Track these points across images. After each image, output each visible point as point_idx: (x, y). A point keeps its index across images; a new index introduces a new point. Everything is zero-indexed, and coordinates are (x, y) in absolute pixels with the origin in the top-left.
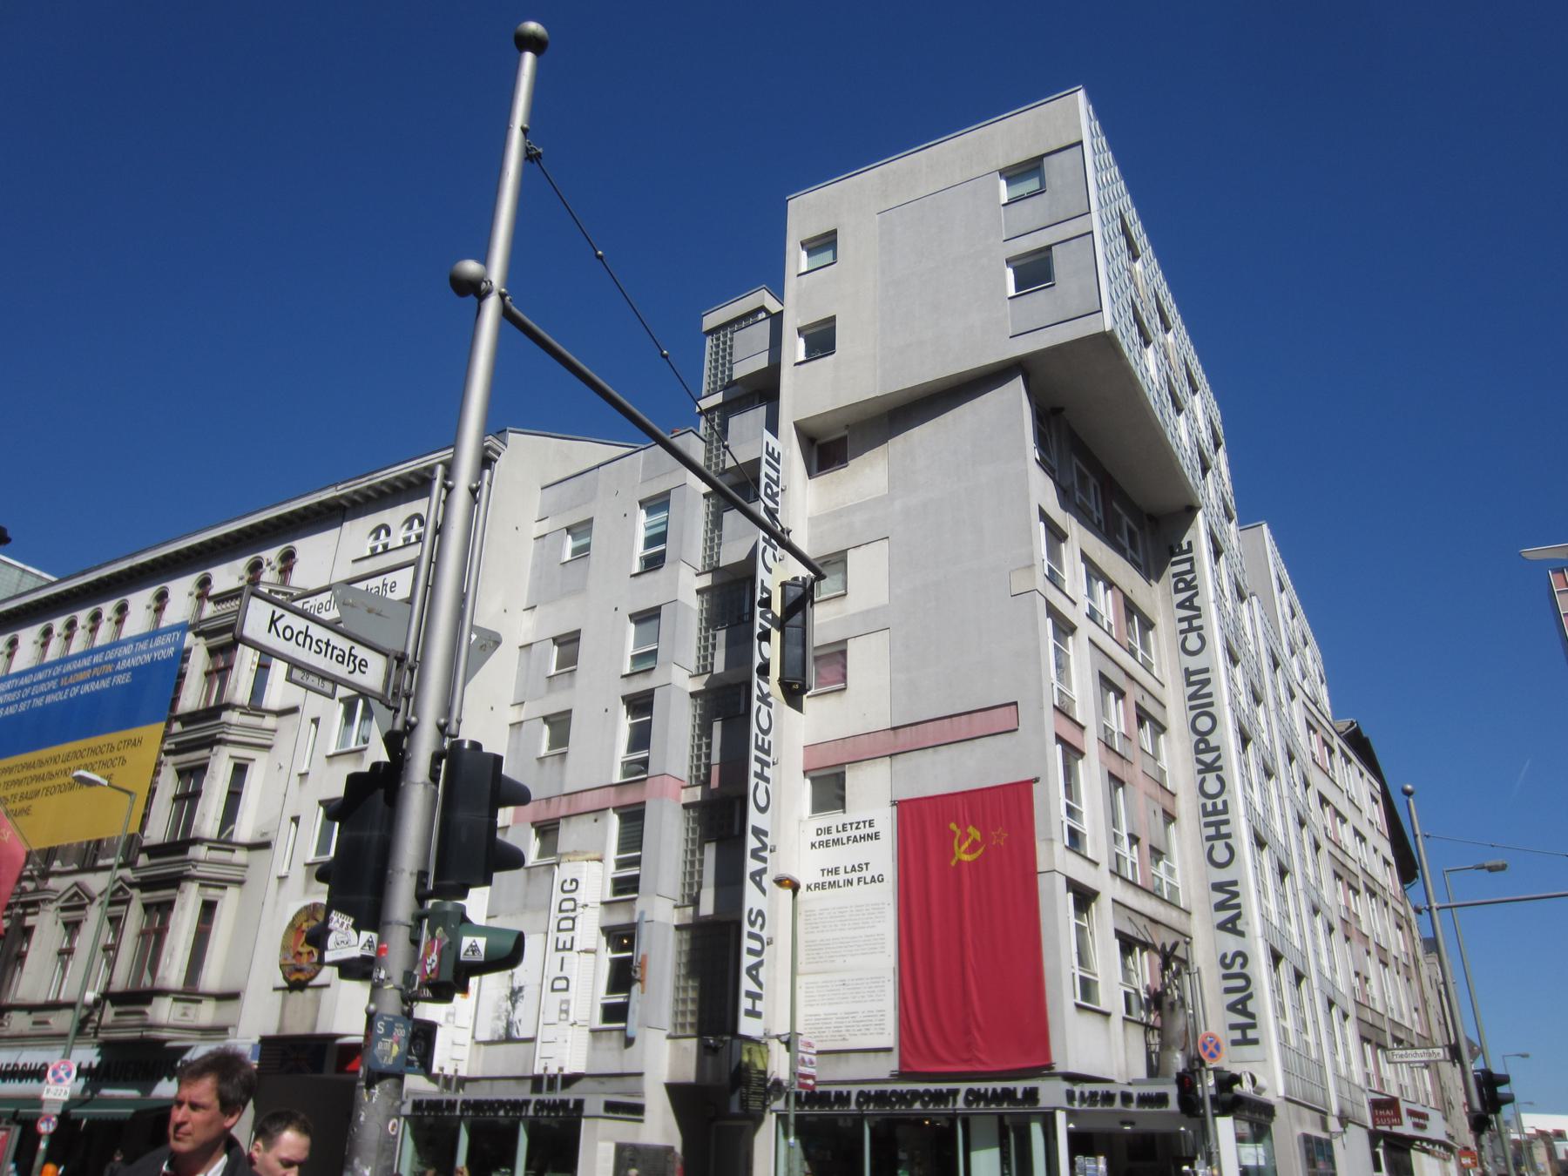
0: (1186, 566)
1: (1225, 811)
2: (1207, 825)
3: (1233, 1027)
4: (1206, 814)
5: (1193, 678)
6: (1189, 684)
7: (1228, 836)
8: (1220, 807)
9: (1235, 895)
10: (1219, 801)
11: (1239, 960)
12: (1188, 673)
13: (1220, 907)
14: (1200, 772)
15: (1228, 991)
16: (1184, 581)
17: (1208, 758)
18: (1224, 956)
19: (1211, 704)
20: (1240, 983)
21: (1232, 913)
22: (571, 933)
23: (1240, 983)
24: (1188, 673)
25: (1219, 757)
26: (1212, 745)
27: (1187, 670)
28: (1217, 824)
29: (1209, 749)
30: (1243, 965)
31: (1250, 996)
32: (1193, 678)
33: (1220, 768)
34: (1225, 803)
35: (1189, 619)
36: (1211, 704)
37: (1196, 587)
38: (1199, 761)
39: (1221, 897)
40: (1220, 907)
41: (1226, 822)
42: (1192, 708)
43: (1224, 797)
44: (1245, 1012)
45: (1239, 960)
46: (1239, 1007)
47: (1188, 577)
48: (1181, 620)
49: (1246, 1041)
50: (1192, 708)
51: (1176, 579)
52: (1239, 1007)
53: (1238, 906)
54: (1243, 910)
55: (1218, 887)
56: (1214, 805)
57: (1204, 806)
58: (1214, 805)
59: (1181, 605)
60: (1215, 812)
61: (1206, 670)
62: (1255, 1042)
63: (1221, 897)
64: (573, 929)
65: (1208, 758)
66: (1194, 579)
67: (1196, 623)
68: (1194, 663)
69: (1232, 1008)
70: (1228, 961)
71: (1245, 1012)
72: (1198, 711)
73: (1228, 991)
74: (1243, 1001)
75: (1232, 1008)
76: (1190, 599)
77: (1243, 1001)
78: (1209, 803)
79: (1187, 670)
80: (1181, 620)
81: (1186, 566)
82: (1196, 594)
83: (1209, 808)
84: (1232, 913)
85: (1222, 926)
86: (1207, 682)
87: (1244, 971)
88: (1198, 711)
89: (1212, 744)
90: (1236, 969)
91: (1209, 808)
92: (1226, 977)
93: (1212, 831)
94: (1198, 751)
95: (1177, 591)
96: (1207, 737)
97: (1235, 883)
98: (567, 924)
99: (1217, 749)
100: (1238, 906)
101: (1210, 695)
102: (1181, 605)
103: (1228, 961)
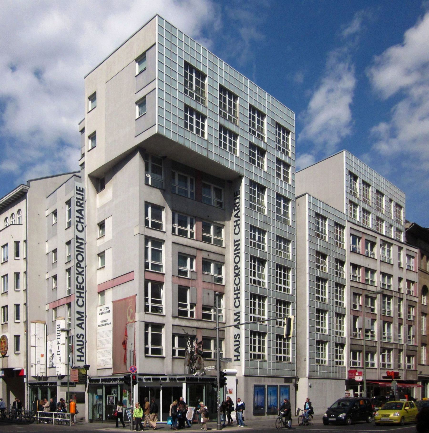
1: (239, 290)
2: (235, 294)
3: (235, 356)
4: (235, 291)
5: (236, 243)
6: (235, 246)
7: (239, 298)
9: (239, 316)
10: (238, 286)
12: (235, 241)
17: (237, 271)
18: (235, 335)
19: (239, 253)
20: (237, 343)
22: (59, 339)
23: (237, 343)
24: (235, 241)
25: (239, 271)
26: (239, 267)
30: (239, 338)
32: (236, 243)
34: (239, 287)
38: (235, 273)
39: (236, 317)
41: (239, 293)
43: (239, 285)
46: (237, 350)
47: (238, 205)
48: (235, 222)
50: (235, 254)
52: (237, 350)
55: (236, 314)
56: (237, 287)
57: (235, 288)
58: (237, 287)
61: (239, 240)
62: (239, 360)
63: (236, 317)
64: (60, 338)
65: (237, 271)
66: (239, 206)
69: (235, 350)
72: (236, 255)
74: (238, 348)
82: (239, 212)
83: (236, 289)
86: (239, 245)
88: (236, 255)
89: (239, 267)
90: (237, 339)
92: (235, 341)
94: (235, 269)
97: (239, 313)
98: (59, 337)
99: (239, 268)
101: (239, 249)
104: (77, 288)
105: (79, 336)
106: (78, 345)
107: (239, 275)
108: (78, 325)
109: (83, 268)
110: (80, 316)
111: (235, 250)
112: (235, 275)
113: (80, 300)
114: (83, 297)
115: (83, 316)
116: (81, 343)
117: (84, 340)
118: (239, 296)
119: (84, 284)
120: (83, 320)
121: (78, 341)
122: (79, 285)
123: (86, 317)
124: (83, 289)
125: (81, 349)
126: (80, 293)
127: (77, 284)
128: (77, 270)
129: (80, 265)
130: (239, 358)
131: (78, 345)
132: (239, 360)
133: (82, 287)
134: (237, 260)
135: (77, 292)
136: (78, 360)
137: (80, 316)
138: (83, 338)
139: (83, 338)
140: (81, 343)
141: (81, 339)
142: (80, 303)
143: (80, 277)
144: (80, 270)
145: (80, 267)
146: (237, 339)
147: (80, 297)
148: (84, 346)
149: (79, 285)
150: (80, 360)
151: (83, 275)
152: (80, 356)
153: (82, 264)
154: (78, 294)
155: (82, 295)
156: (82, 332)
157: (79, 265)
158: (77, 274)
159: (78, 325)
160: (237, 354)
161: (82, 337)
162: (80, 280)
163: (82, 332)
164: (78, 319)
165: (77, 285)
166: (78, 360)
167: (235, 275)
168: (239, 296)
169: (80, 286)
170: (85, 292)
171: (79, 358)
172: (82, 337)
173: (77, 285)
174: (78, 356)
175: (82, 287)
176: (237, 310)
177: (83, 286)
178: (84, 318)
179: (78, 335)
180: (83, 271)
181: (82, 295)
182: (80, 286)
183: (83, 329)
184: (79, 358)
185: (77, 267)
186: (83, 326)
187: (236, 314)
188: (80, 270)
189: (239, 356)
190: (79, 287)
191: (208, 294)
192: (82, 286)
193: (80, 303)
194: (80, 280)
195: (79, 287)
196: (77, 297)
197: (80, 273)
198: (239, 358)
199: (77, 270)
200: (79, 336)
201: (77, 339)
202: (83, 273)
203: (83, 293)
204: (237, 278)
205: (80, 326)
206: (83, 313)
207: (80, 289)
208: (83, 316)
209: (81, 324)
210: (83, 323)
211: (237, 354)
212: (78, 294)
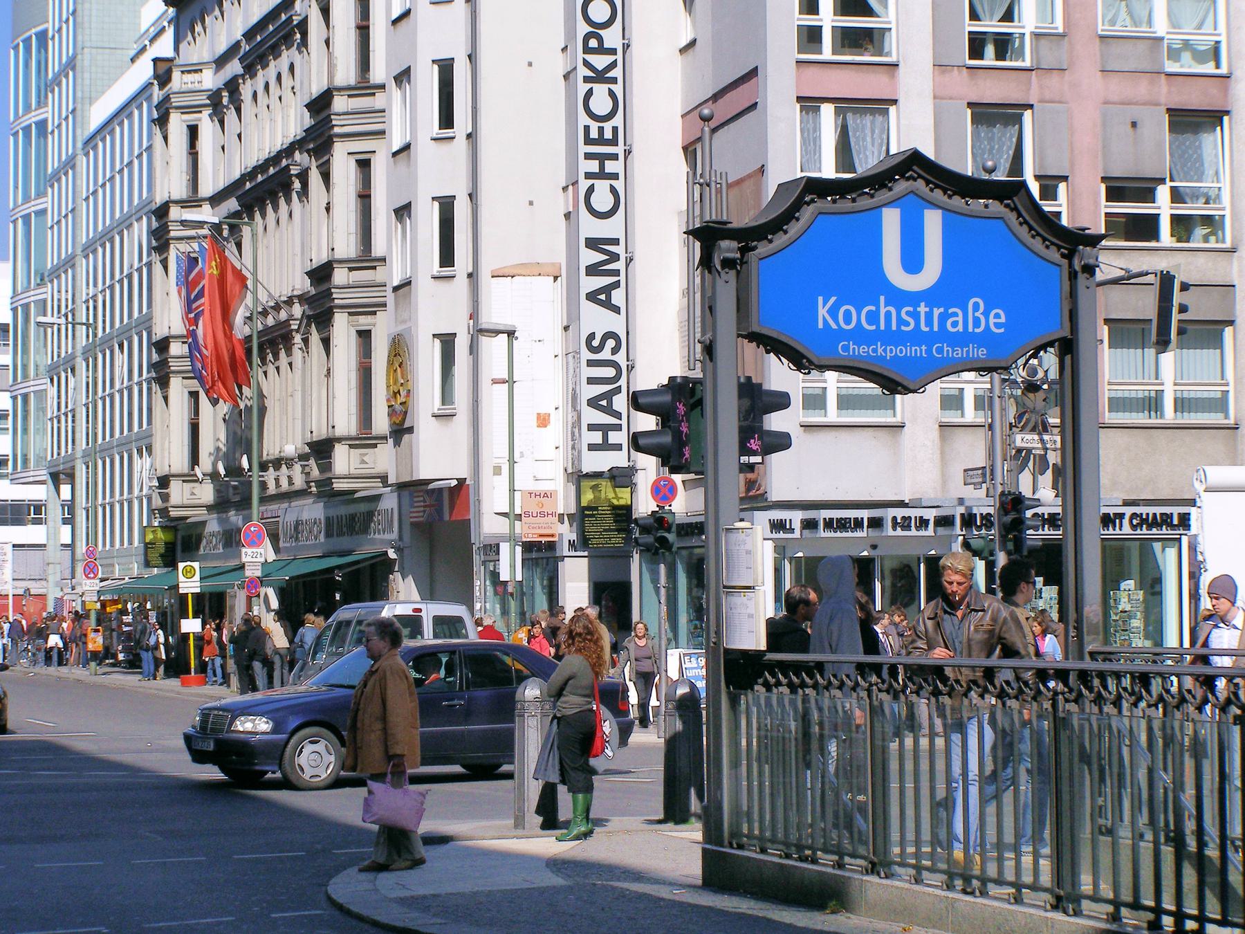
104: (588, 141)
105: (596, 343)
106: (591, 381)
108: (592, 297)
109: (613, 51)
110: (605, 257)
113: (602, 186)
114: (615, 176)
115: (615, 257)
116: (610, 372)
117: (620, 358)
119: (618, 121)
120: (616, 273)
121: (591, 363)
122: (594, 127)
123: (629, 261)
124: (614, 142)
125: (609, 396)
126: (602, 158)
127: (589, 122)
128: (587, 64)
129: (600, 39)
131: (591, 381)
133: (608, 135)
135: (588, 156)
136: (592, 447)
137: (605, 257)
138: (615, 351)
139: (615, 351)
140: (610, 372)
141: (606, 354)
142: (602, 200)
143: (600, 90)
144: (600, 62)
145: (601, 50)
147: (602, 175)
148: (623, 382)
149: (594, 127)
150: (605, 446)
151: (614, 80)
152: (605, 429)
153: (611, 37)
154: (594, 166)
155: (610, 167)
156: (616, 323)
157: (593, 43)
158: (587, 79)
159: (592, 297)
161: (611, 343)
162: (601, 104)
163: (616, 323)
164: (593, 270)
165: (587, 128)
166: (592, 447)
169: (601, 130)
170: (628, 153)
171: (597, 437)
172: (611, 343)
173: (587, 128)
174: (592, 427)
175: (608, 135)
177: (615, 129)
178: (620, 265)
179: (592, 336)
180: (613, 65)
181: (610, 167)
182: (601, 130)
183: (617, 310)
184: (597, 437)
185: (587, 50)
186: (618, 297)
188: (600, 62)
190: (594, 134)
191: (1134, 125)
192: (608, 127)
193: (602, 200)
194: (601, 104)
195: (594, 134)
196: (589, 176)
197: (600, 76)
199: (587, 64)
200: (596, 343)
201: (586, 355)
202: (617, 73)
203: (614, 157)
205: (601, 298)
206: (615, 242)
207: (601, 141)
208: (615, 257)
209: (608, 289)
210: (616, 285)
212: (594, 166)
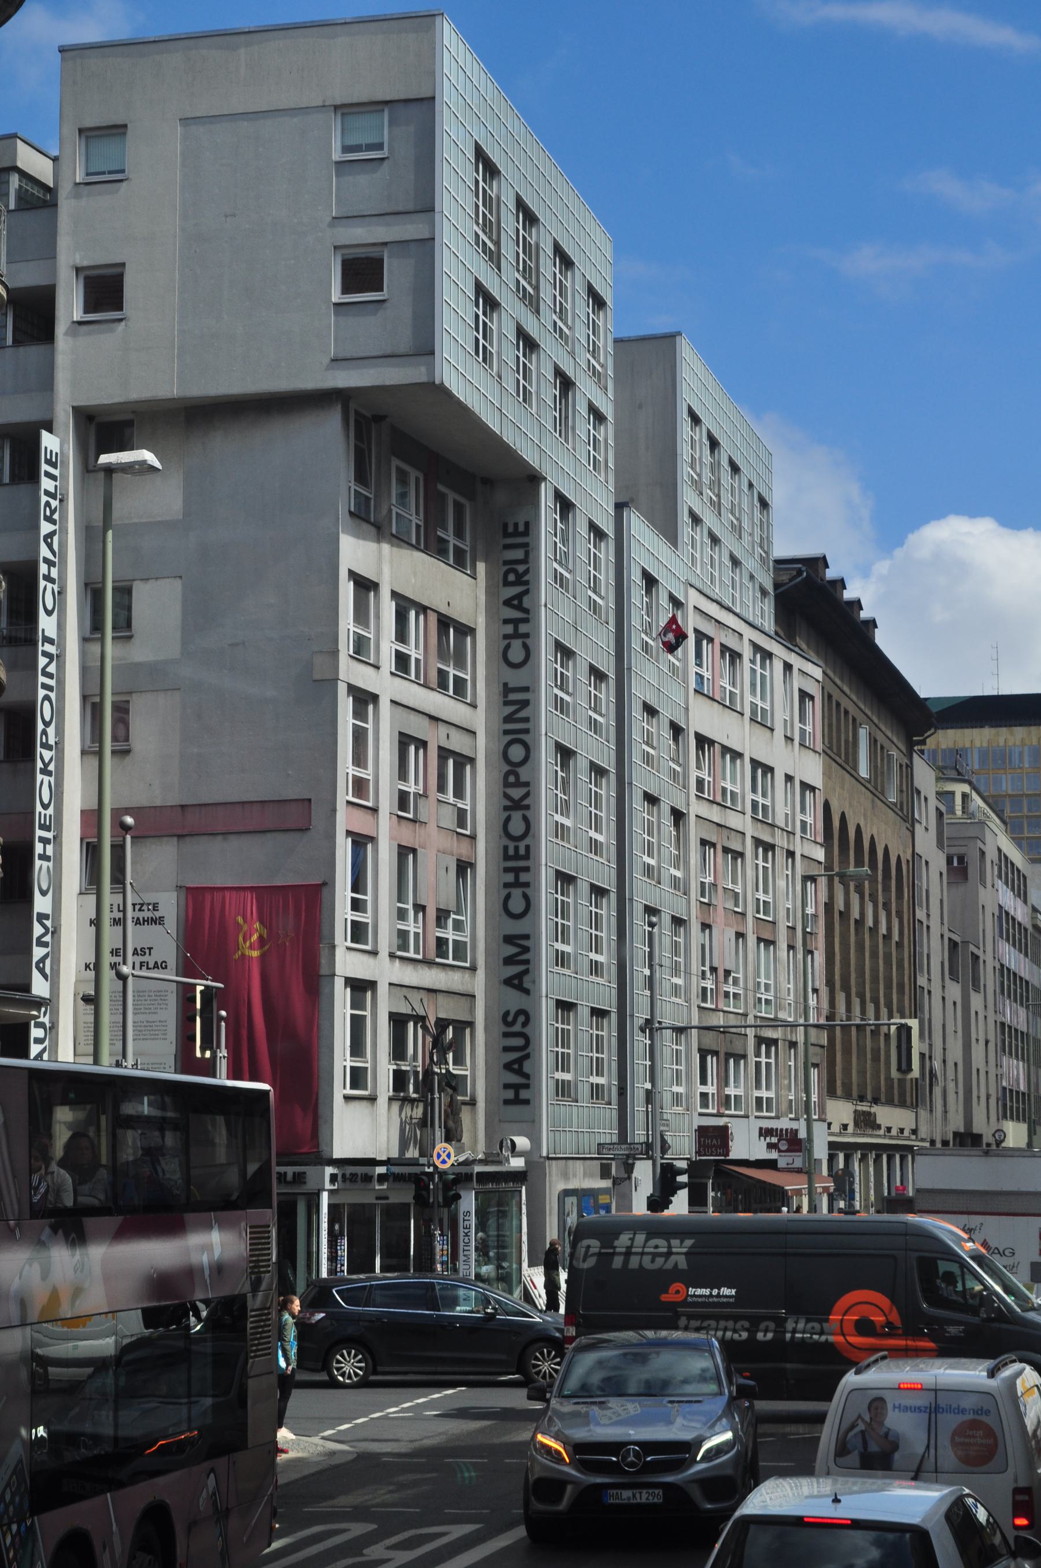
0: (519, 554)
1: (527, 856)
2: (507, 870)
4: (506, 857)
5: (513, 697)
6: (506, 703)
8: (522, 851)
10: (522, 846)
11: (521, 1019)
12: (507, 689)
13: (508, 961)
14: (506, 808)
15: (506, 1049)
16: (515, 571)
17: (516, 793)
18: (507, 1014)
19: (527, 731)
20: (519, 1042)
21: (521, 968)
23: (519, 1042)
25: (527, 795)
27: (505, 685)
28: (517, 871)
29: (518, 784)
30: (525, 1024)
31: (527, 1056)
32: (513, 697)
33: (527, 807)
34: (528, 848)
35: (516, 622)
36: (527, 731)
37: (527, 583)
38: (506, 796)
39: (512, 950)
40: (508, 961)
41: (527, 869)
42: (506, 732)
43: (526, 842)
44: (520, 1072)
45: (521, 1019)
48: (506, 622)
49: (517, 1101)
50: (506, 732)
51: (507, 567)
53: (527, 962)
54: (531, 967)
55: (509, 939)
56: (516, 848)
57: (506, 848)
58: (516, 848)
59: (507, 603)
60: (517, 857)
61: (526, 689)
62: (527, 1102)
63: (512, 950)
65: (516, 793)
67: (523, 628)
68: (515, 678)
70: (510, 1019)
71: (520, 1072)
73: (506, 1049)
74: (520, 1061)
75: (508, 1067)
76: (520, 596)
77: (520, 1061)
78: (511, 845)
79: (505, 685)
80: (506, 622)
81: (519, 554)
83: (511, 852)
84: (521, 968)
85: (508, 982)
86: (525, 703)
87: (525, 1030)
89: (523, 779)
90: (517, 1028)
91: (511, 852)
92: (506, 1035)
93: (510, 878)
94: (506, 784)
95: (506, 583)
96: (517, 769)
97: (527, 937)
99: (527, 784)
100: (527, 962)
101: (526, 720)
102: (507, 603)
103: (510, 1019)
107: (527, 807)
111: (508, 719)
112: (508, 803)
118: (524, 877)
130: (524, 1094)
132: (527, 1102)
134: (517, 753)
146: (517, 1028)
160: (515, 1079)
167: (508, 803)
168: (524, 877)
176: (515, 928)
187: (509, 939)
189: (527, 1086)
198: (524, 1094)
204: (517, 816)
211: (515, 1079)
